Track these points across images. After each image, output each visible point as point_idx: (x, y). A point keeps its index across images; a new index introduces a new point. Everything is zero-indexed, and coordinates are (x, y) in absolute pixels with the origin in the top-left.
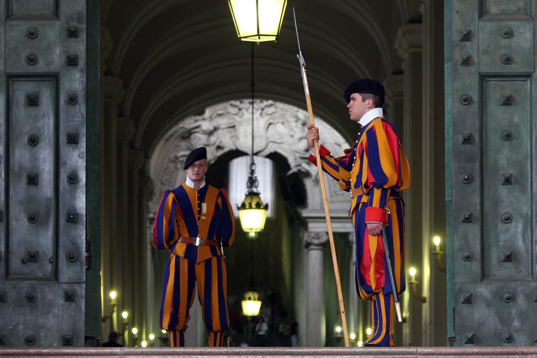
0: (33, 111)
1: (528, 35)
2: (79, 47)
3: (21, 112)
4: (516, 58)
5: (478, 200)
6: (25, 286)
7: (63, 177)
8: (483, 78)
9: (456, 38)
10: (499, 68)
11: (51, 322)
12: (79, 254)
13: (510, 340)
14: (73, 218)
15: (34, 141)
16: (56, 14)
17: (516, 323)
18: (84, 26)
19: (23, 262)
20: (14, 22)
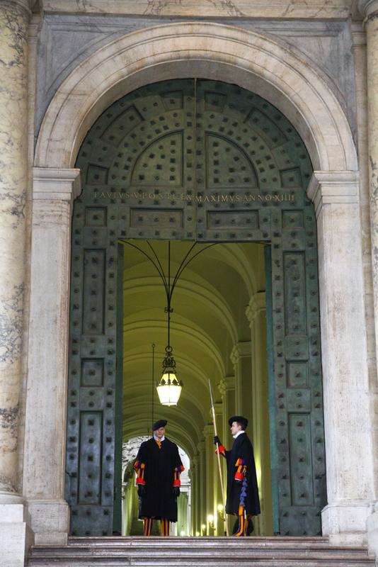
0: (91, 427)
1: (308, 395)
2: (112, 399)
3: (86, 428)
4: (304, 405)
5: (288, 469)
6: (85, 507)
7: (104, 457)
8: (289, 414)
9: (277, 396)
10: (296, 410)
11: (98, 524)
12: (110, 493)
13: (305, 534)
14: (108, 476)
15: (91, 441)
16: (102, 384)
17: (308, 526)
18: (114, 390)
19: (86, 496)
20: (84, 388)
